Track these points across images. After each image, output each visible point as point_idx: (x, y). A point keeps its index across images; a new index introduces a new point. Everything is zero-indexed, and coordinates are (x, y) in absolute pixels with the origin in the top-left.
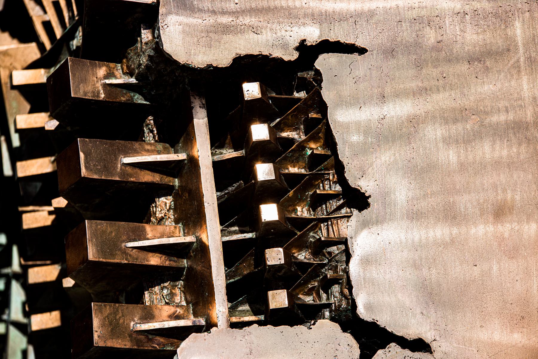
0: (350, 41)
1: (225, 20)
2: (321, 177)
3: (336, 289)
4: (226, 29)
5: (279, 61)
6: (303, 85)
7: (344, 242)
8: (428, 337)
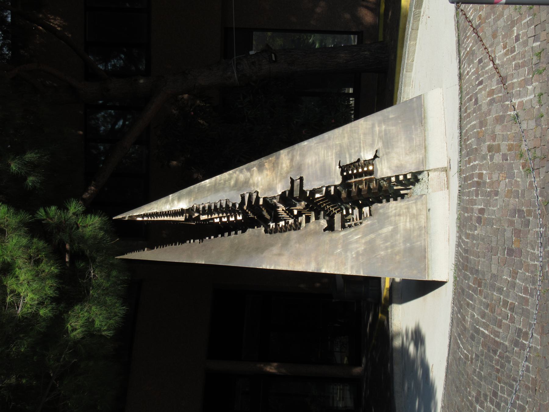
1: (336, 177)
2: (356, 165)
3: (370, 162)
4: (337, 177)
5: (341, 170)
6: (344, 168)
7: (364, 161)
8: (376, 150)
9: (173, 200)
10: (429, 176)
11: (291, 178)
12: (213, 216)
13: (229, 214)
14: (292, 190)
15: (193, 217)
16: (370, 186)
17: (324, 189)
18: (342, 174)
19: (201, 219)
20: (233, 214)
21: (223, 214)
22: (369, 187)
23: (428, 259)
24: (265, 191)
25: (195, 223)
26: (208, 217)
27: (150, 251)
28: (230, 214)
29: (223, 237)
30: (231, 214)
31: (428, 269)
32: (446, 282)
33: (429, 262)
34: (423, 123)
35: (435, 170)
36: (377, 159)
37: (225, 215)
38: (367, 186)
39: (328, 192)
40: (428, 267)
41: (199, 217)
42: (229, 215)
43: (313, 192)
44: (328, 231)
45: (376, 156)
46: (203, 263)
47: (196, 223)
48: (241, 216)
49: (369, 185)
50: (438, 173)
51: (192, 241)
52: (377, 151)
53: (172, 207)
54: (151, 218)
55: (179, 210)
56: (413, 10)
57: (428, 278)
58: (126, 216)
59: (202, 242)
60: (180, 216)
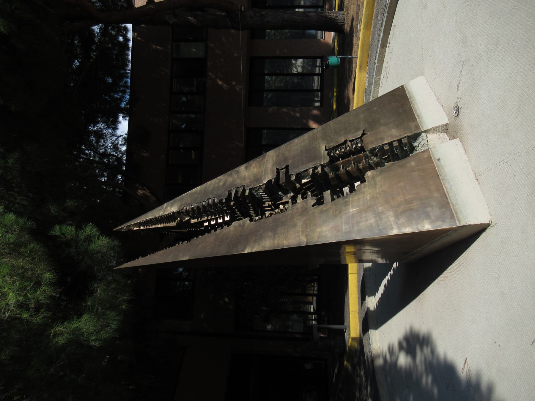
0: (325, 147)
3: (358, 141)
8: (363, 130)
9: (166, 207)
10: (428, 138)
11: (276, 169)
12: (203, 219)
13: (217, 216)
14: (277, 178)
15: (184, 221)
16: (359, 167)
17: (311, 170)
18: (329, 154)
19: (191, 223)
20: (221, 215)
21: (212, 216)
22: (358, 167)
23: (453, 204)
24: (251, 182)
25: (186, 230)
26: (198, 220)
27: (143, 258)
28: (218, 215)
29: (209, 234)
30: (219, 215)
31: (456, 214)
32: (489, 225)
33: (456, 207)
34: (410, 101)
35: (434, 130)
36: (364, 136)
37: (213, 217)
38: (356, 165)
39: (314, 175)
40: (455, 212)
41: (189, 220)
42: (218, 218)
43: (299, 177)
44: (317, 206)
45: (363, 134)
46: (187, 258)
47: (187, 230)
48: (229, 217)
49: (357, 165)
50: (438, 134)
51: (181, 243)
52: (364, 131)
53: (164, 212)
54: (147, 227)
55: (171, 213)
56: (374, 77)
57: (460, 223)
58: (124, 227)
59: (190, 242)
60: (172, 222)
